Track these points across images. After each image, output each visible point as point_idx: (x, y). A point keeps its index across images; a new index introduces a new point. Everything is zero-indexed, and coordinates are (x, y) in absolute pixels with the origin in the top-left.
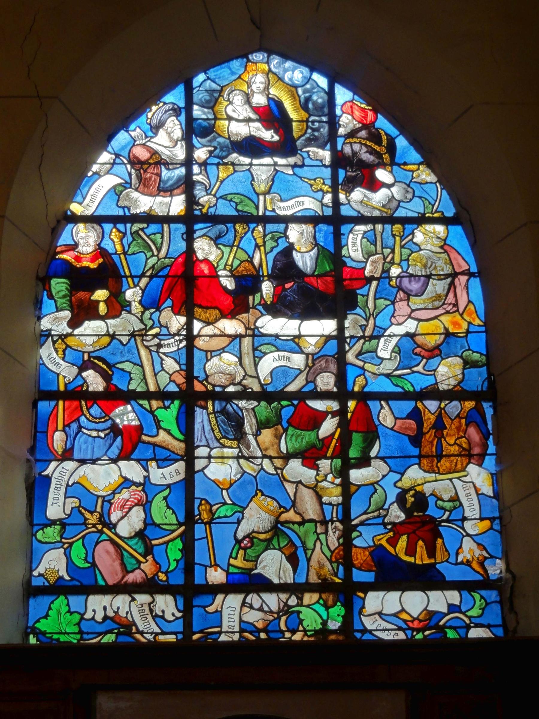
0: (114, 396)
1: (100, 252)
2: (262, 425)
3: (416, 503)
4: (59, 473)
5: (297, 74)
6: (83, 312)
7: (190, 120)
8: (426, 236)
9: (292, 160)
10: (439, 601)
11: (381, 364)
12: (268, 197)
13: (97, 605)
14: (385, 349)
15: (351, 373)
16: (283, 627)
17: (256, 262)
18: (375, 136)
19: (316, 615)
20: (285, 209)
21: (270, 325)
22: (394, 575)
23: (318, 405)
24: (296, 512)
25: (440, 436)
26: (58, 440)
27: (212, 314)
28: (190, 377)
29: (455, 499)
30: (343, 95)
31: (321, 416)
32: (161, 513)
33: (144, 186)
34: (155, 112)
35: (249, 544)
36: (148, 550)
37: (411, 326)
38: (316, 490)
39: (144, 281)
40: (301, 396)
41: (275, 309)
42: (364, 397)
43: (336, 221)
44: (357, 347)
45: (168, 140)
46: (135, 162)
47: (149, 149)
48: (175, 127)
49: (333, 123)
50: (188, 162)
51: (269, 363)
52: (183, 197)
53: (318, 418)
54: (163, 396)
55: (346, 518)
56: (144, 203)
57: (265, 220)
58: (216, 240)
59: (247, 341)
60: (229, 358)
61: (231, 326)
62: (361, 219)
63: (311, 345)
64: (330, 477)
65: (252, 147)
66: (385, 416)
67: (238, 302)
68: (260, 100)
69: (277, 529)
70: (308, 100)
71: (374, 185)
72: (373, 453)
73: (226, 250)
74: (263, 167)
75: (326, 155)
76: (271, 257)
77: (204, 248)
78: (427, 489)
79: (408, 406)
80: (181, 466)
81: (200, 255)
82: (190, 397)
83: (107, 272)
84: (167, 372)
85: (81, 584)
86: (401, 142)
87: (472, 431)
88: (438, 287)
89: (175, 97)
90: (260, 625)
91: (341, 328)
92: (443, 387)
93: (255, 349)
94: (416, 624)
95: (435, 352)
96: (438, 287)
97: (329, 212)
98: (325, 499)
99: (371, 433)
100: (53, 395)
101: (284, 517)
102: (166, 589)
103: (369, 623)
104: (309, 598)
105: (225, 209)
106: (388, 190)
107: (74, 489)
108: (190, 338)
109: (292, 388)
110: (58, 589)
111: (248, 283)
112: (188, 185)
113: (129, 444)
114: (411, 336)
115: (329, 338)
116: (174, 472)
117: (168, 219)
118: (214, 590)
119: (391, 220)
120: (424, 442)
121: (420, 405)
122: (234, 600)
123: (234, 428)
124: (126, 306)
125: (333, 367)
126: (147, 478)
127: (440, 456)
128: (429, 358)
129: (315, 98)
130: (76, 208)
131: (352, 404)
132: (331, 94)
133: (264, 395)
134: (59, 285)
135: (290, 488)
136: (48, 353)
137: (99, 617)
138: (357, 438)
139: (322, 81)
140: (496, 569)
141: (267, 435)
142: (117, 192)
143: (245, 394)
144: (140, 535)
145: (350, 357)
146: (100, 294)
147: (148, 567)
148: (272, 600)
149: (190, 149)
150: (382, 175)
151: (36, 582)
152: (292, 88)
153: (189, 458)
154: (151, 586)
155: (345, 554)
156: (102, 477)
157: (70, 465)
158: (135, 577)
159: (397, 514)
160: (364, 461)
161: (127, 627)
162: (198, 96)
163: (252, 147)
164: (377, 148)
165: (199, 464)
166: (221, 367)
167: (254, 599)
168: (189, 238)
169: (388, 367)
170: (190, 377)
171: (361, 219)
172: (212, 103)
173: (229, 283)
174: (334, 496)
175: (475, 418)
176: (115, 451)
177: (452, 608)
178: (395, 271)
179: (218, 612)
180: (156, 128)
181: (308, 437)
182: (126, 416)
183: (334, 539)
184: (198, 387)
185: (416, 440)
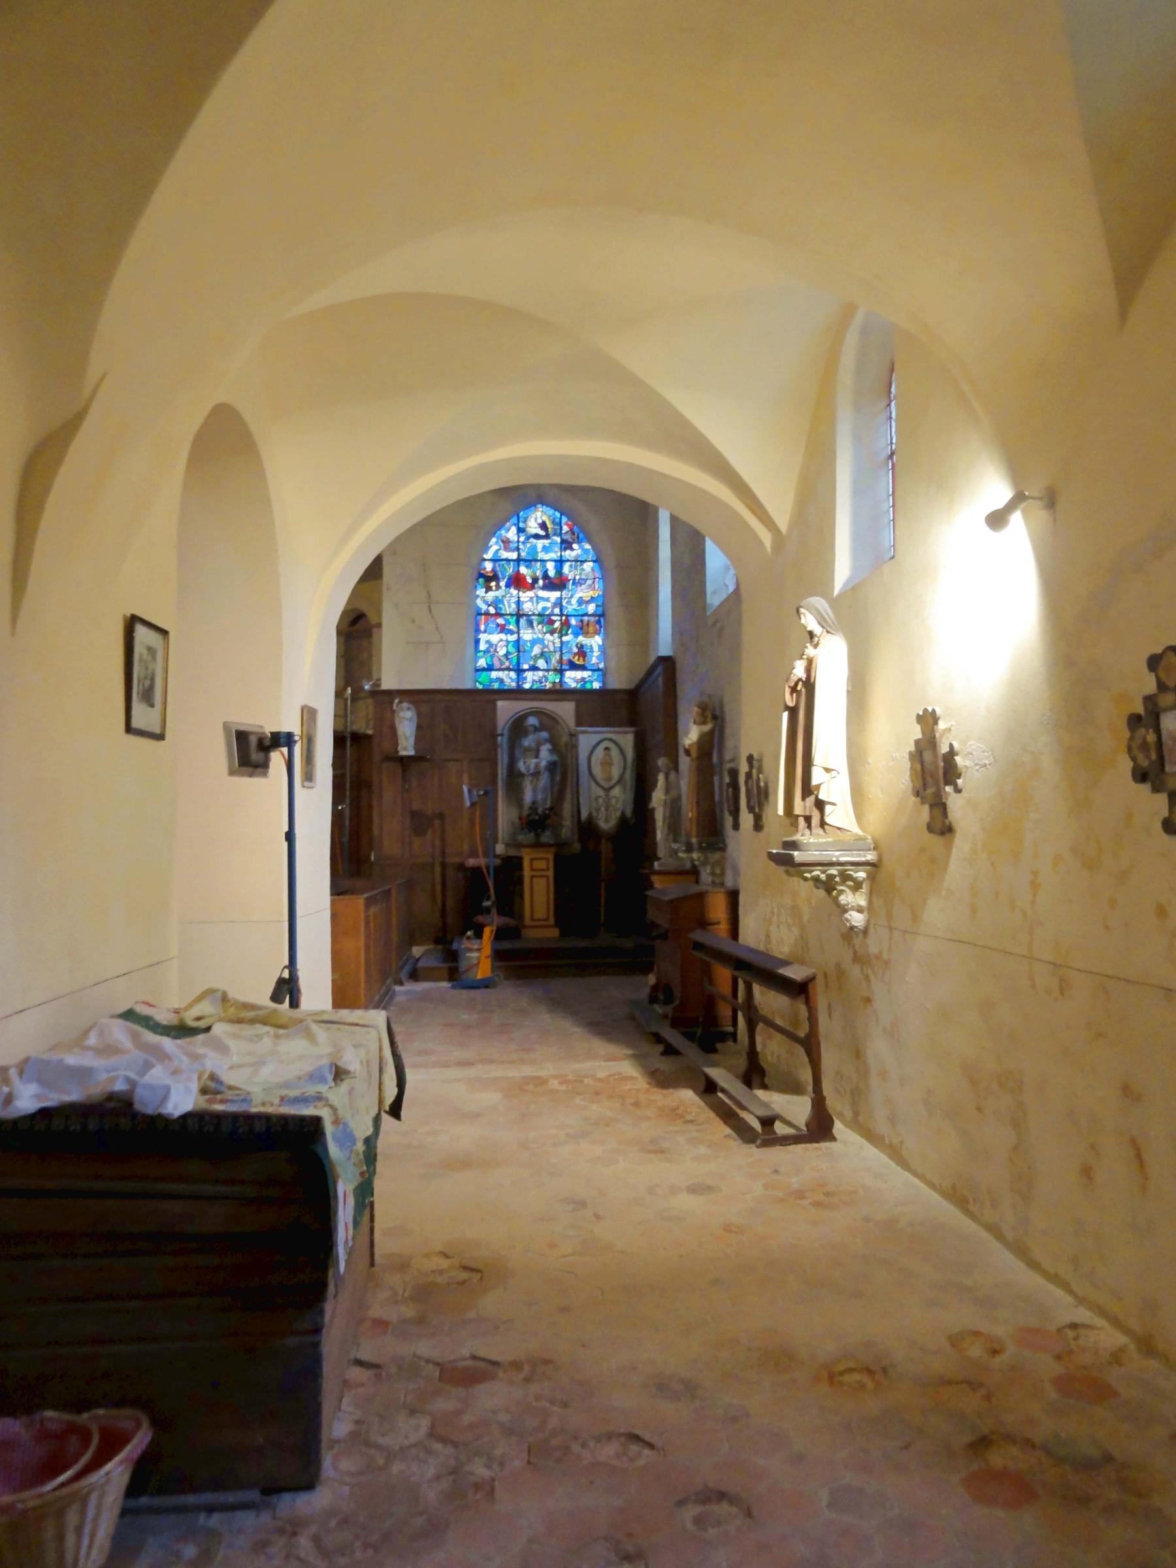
0: (498, 614)
1: (493, 570)
3: (581, 647)
4: (483, 637)
5: (551, 511)
6: (489, 589)
8: (588, 566)
10: (586, 674)
11: (572, 607)
13: (494, 674)
14: (574, 601)
18: (573, 534)
19: (553, 677)
20: (546, 557)
21: (542, 593)
22: (573, 666)
23: (554, 618)
26: (482, 628)
30: (564, 519)
32: (511, 649)
33: (507, 549)
35: (536, 658)
37: (581, 594)
38: (554, 643)
40: (550, 615)
41: (544, 588)
42: (567, 616)
43: (560, 562)
45: (512, 534)
48: (514, 529)
49: (561, 529)
51: (541, 605)
54: (511, 615)
56: (505, 555)
57: (541, 561)
58: (527, 567)
61: (531, 594)
63: (553, 600)
65: (537, 536)
66: (573, 621)
67: (532, 587)
68: (540, 521)
69: (542, 654)
71: (572, 549)
74: (540, 543)
75: (558, 539)
77: (523, 570)
82: (519, 615)
83: (495, 577)
85: (490, 668)
86: (581, 536)
88: (589, 582)
89: (514, 520)
95: (588, 602)
96: (589, 582)
100: (481, 614)
103: (566, 680)
106: (576, 551)
107: (488, 642)
110: (484, 669)
111: (535, 580)
112: (518, 549)
113: (503, 629)
116: (515, 637)
119: (576, 561)
120: (583, 629)
130: (485, 556)
133: (539, 615)
134: (481, 580)
136: (479, 602)
139: (558, 514)
140: (601, 666)
142: (497, 551)
143: (534, 614)
145: (564, 603)
146: (493, 584)
147: (507, 664)
148: (541, 673)
150: (575, 546)
152: (549, 517)
153: (519, 633)
154: (508, 669)
155: (561, 661)
156: (495, 638)
159: (575, 650)
160: (567, 634)
161: (501, 681)
163: (537, 536)
166: (527, 607)
172: (525, 522)
173: (529, 580)
175: (598, 622)
180: (509, 530)
182: (500, 621)
183: (558, 656)
185: (581, 628)
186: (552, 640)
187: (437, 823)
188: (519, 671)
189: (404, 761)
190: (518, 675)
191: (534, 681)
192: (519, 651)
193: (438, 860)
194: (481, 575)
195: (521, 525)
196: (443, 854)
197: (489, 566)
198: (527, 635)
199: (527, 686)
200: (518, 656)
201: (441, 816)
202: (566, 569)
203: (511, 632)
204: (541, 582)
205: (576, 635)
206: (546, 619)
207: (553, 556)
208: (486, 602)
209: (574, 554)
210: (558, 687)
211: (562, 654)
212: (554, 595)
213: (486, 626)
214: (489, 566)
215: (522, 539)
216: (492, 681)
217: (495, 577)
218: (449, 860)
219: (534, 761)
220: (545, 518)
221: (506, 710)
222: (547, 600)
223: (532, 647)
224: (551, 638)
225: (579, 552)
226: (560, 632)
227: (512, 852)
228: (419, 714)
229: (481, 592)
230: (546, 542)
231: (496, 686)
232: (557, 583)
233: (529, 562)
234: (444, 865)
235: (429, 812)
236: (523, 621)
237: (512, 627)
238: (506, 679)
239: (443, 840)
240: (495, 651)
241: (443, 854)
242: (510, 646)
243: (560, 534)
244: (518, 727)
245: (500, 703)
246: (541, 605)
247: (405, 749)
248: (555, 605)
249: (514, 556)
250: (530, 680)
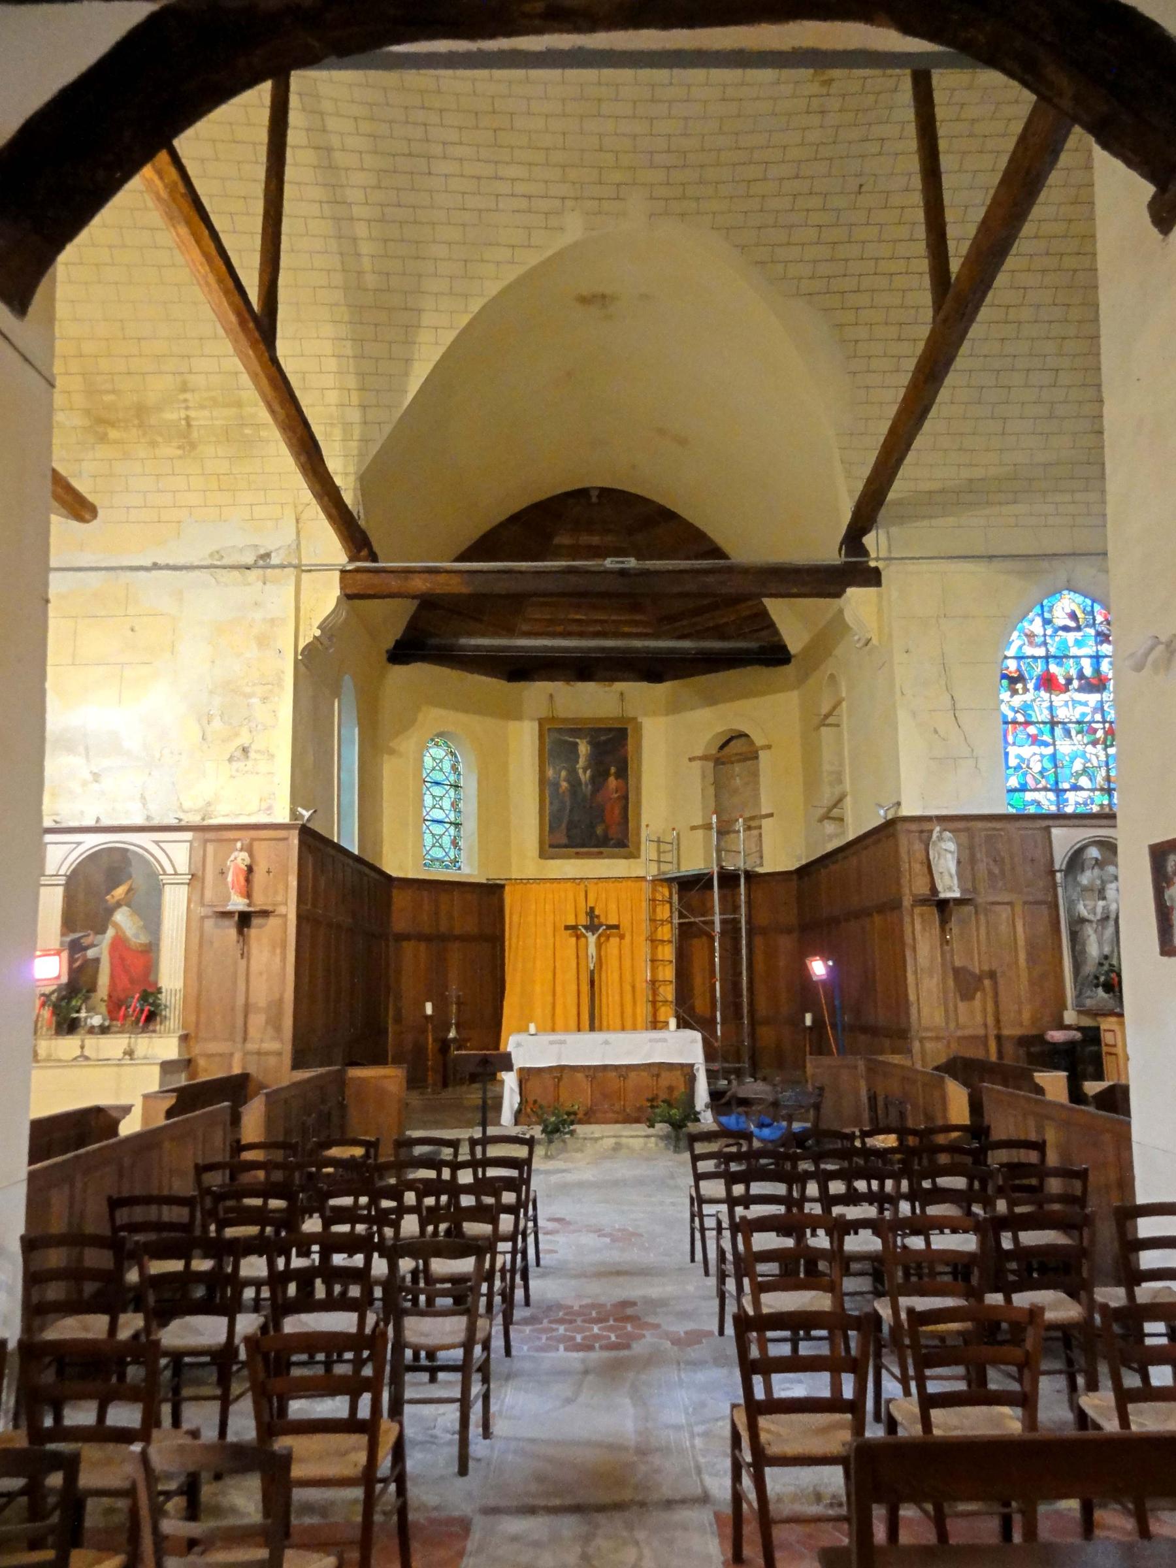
0: (1027, 723)
1: (1018, 670)
2: (1078, 733)
5: (1079, 599)
6: (1015, 692)
9: (1081, 634)
13: (1029, 796)
19: (1101, 799)
23: (1095, 725)
26: (1010, 739)
28: (1052, 717)
30: (1097, 607)
32: (1048, 765)
33: (1031, 643)
34: (1031, 615)
35: (1078, 775)
36: (1043, 777)
40: (1090, 722)
41: (1080, 690)
43: (1097, 658)
45: (1037, 627)
46: (1026, 635)
48: (1038, 621)
49: (1094, 619)
50: (1045, 635)
53: (1095, 731)
54: (1044, 723)
55: (1107, 764)
56: (1029, 651)
57: (1073, 657)
58: (1058, 664)
59: (1070, 703)
60: (1065, 708)
61: (1065, 697)
62: (1107, 656)
63: (1092, 704)
65: (1066, 629)
67: (1065, 689)
69: (1085, 771)
74: (1071, 637)
75: (1092, 631)
77: (1053, 668)
82: (1053, 723)
83: (1020, 678)
84: (1045, 716)
85: (1023, 789)
102: (1050, 790)
104: (1097, 793)
105: (1059, 654)
107: (1018, 756)
108: (1051, 702)
109: (1086, 720)
111: (1069, 681)
112: (1045, 644)
113: (1034, 740)
116: (1050, 750)
117: (1040, 657)
118: (1066, 791)
122: (1073, 793)
123: (1068, 733)
124: (1028, 690)
130: (1008, 653)
131: (1107, 725)
132: (1092, 607)
133: (1078, 722)
134: (1005, 682)
135: (1088, 755)
136: (1004, 708)
138: (1109, 737)
139: (1089, 602)
141: (1080, 736)
142: (1020, 648)
143: (1070, 722)
144: (1041, 773)
145: (1106, 708)
146: (1019, 686)
147: (1043, 782)
148: (1085, 794)
152: (1079, 605)
153: (1054, 744)
154: (1045, 789)
156: (1027, 751)
158: (1040, 786)
160: (1112, 745)
161: (1038, 804)
162: (1046, 609)
163: (1066, 629)
166: (1062, 714)
167: (1078, 793)
168: (1047, 663)
170: (1052, 717)
171: (1107, 656)
172: (1050, 611)
173: (1062, 681)
174: (1103, 758)
180: (1032, 621)
181: (1092, 737)
182: (1032, 730)
183: (1103, 772)
186: (1097, 754)
187: (987, 982)
189: (943, 906)
190: (1058, 796)
191: (1077, 803)
192: (1056, 766)
193: (992, 1032)
194: (1004, 676)
195: (1047, 615)
196: (998, 1021)
197: (1012, 665)
198: (1065, 747)
199: (1069, 810)
200: (1056, 773)
201: (992, 975)
203: (1046, 744)
204: (1076, 683)
206: (1084, 726)
207: (1091, 651)
208: (1012, 709)
210: (1107, 810)
211: (1108, 771)
212: (1093, 698)
213: (1015, 738)
215: (1049, 631)
216: (1026, 804)
217: (1020, 678)
218: (1006, 1032)
219: (1101, 903)
220: (1075, 607)
221: (1063, 840)
222: (1086, 704)
223: (1072, 762)
226: (1104, 742)
227: (1087, 1022)
228: (959, 845)
229: (1005, 695)
230: (1078, 635)
231: (1032, 810)
232: (1097, 684)
233: (1060, 659)
234: (999, 1038)
235: (977, 971)
236: (1058, 730)
237: (1047, 738)
238: (1044, 802)
239: (996, 1003)
240: (1028, 767)
241: (998, 1021)
242: (1045, 760)
244: (1076, 861)
245: (1054, 831)
246: (1080, 709)
247: (950, 889)
248: (1095, 711)
249: (1041, 652)
250: (1073, 803)
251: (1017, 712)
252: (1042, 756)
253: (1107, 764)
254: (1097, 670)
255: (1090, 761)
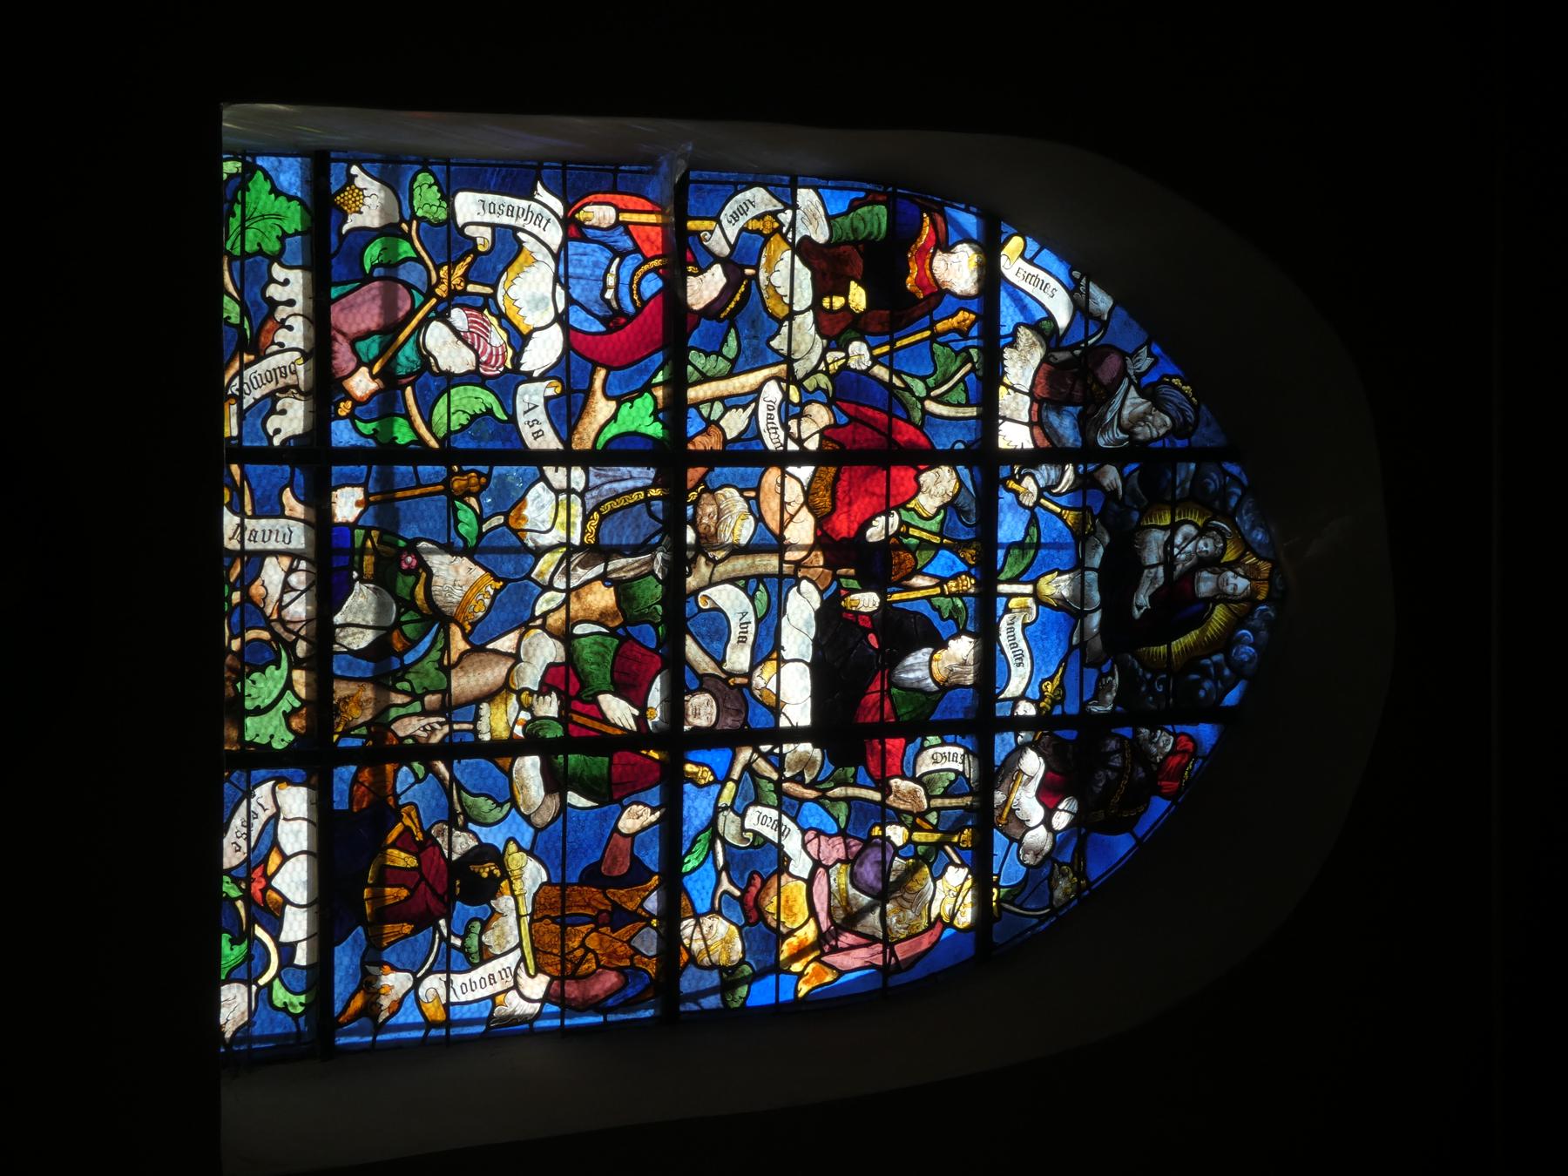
1: (939, 293)
3: (477, 882)
7: (1173, 457)
11: (730, 809)
12: (1030, 601)
14: (761, 819)
15: (718, 757)
16: (251, 635)
17: (918, 581)
18: (1138, 798)
21: (802, 606)
24: (463, 655)
25: (597, 922)
26: (599, 214)
27: (823, 500)
28: (710, 459)
29: (485, 956)
31: (640, 702)
37: (801, 865)
39: (881, 372)
40: (676, 666)
41: (831, 617)
44: (763, 766)
47: (1116, 383)
52: (1029, 445)
55: (452, 750)
60: (742, 530)
61: (802, 530)
63: (764, 679)
64: (525, 716)
68: (1206, 585)
70: (1204, 672)
72: (574, 799)
73: (933, 525)
76: (924, 609)
78: (505, 903)
79: (651, 858)
80: (551, 442)
81: (927, 478)
83: (901, 307)
86: (1122, 844)
87: (611, 979)
90: (256, 590)
91: (796, 735)
92: (687, 927)
93: (760, 578)
94: (257, 887)
97: (1002, 711)
98: (484, 706)
99: (611, 794)
101: (456, 632)
107: (508, 244)
108: (782, 459)
109: (692, 649)
111: (880, 565)
114: (783, 863)
115: (776, 710)
120: (592, 889)
121: (655, 880)
125: (729, 722)
126: (529, 377)
127: (565, 922)
128: (741, 900)
129: (1207, 684)
134: (877, 218)
135: (506, 643)
137: (274, 291)
149: (1115, 456)
151: (336, 170)
153: (566, 457)
157: (554, 235)
160: (555, 782)
164: (1116, 799)
165: (557, 476)
169: (729, 826)
176: (578, 318)
177: (287, 951)
178: (897, 834)
179: (279, 512)
184: (694, 474)
185: (593, 876)
188: (314, 463)
202: (944, 758)
204: (867, 601)
205: (550, 843)
206: (656, 634)
209: (1027, 803)
211: (421, 752)
214: (958, 270)
222: (768, 648)
224: (531, 676)
225: (1038, 837)
232: (862, 708)
240: (456, 298)
243: (1132, 710)
248: (734, 692)
251: (733, 266)
252: (515, 376)
253: (452, 750)
254: (926, 716)
255: (477, 649)
